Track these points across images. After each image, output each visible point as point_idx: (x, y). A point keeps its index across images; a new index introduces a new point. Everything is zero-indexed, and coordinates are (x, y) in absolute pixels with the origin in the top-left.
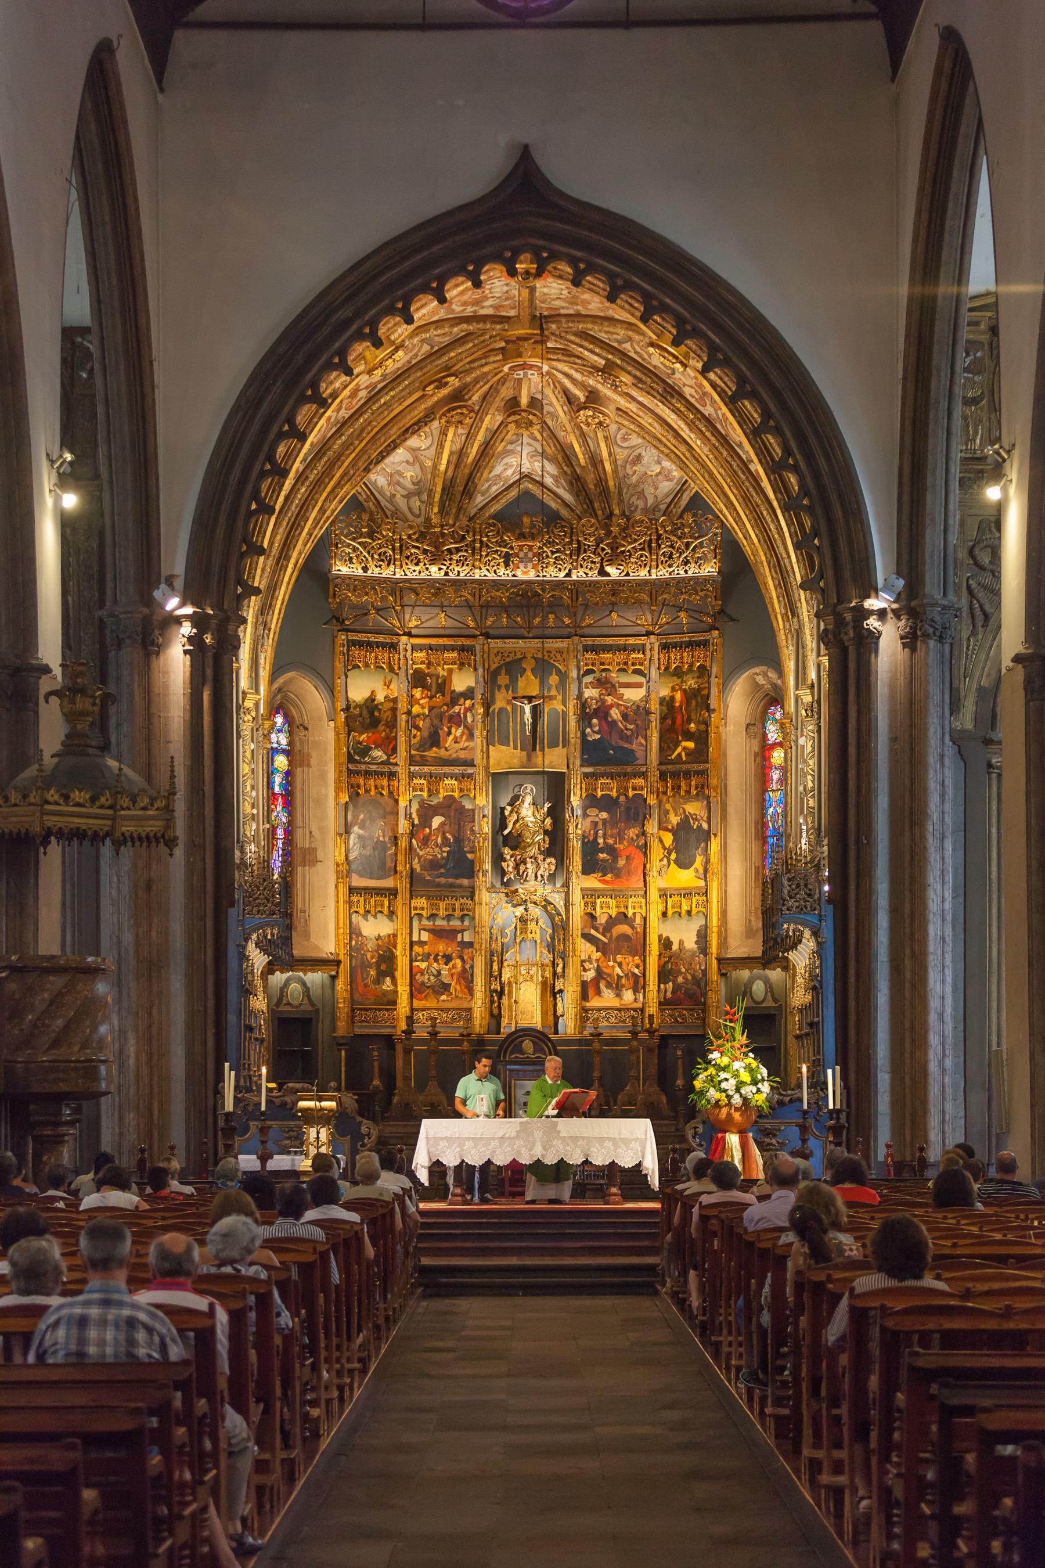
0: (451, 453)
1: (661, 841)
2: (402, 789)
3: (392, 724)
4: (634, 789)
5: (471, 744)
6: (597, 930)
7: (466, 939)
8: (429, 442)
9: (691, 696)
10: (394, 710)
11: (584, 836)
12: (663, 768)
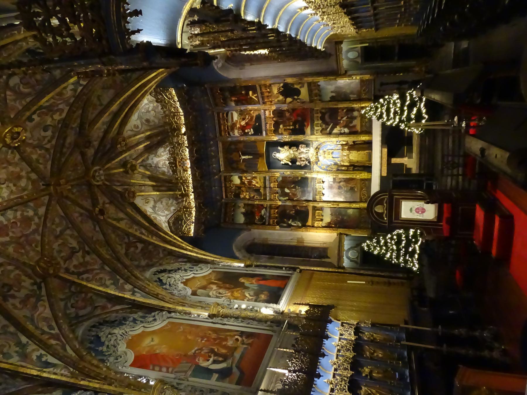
1: (290, 102)
3: (253, 206)
4: (270, 115)
5: (258, 177)
6: (328, 128)
7: (332, 180)
10: (248, 205)
11: (290, 134)
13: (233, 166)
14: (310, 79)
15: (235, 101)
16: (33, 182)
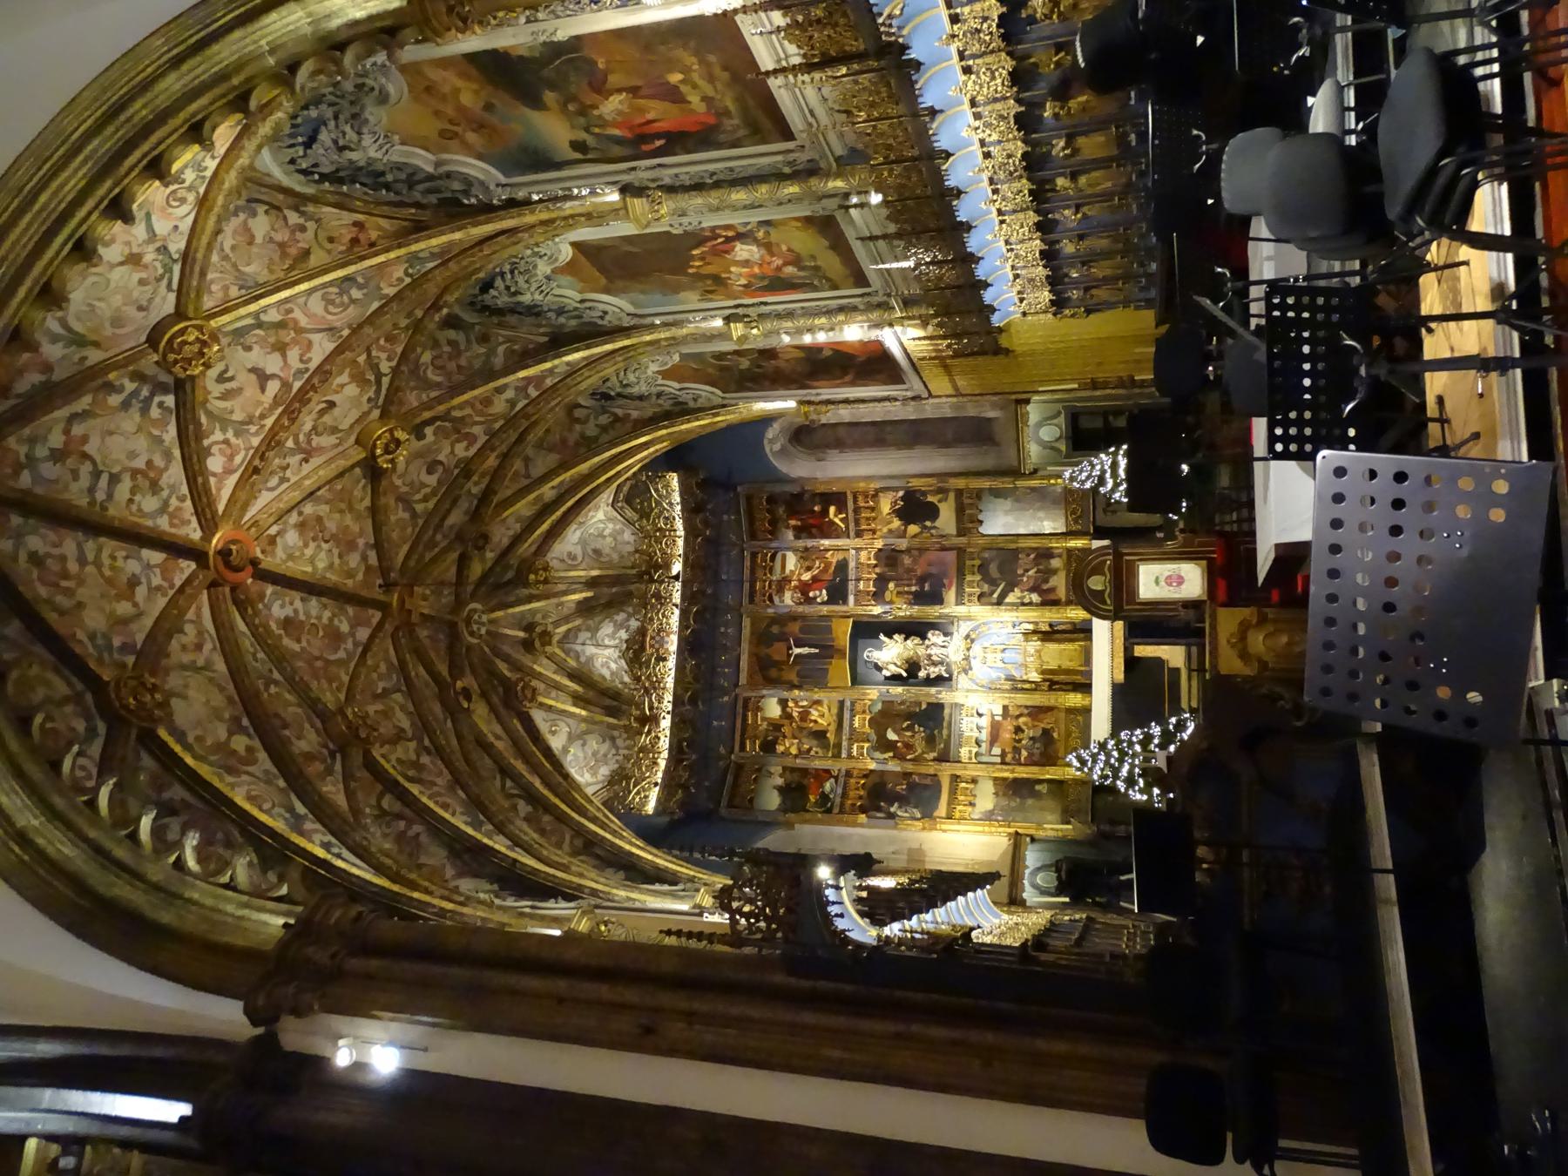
0: (575, 705)
1: (915, 536)
2: (860, 766)
3: (804, 772)
5: (826, 702)
8: (562, 724)
9: (793, 513)
10: (793, 770)
11: (910, 604)
12: (852, 534)
13: (768, 673)
14: (960, 483)
15: (795, 528)
16: (368, 569)
